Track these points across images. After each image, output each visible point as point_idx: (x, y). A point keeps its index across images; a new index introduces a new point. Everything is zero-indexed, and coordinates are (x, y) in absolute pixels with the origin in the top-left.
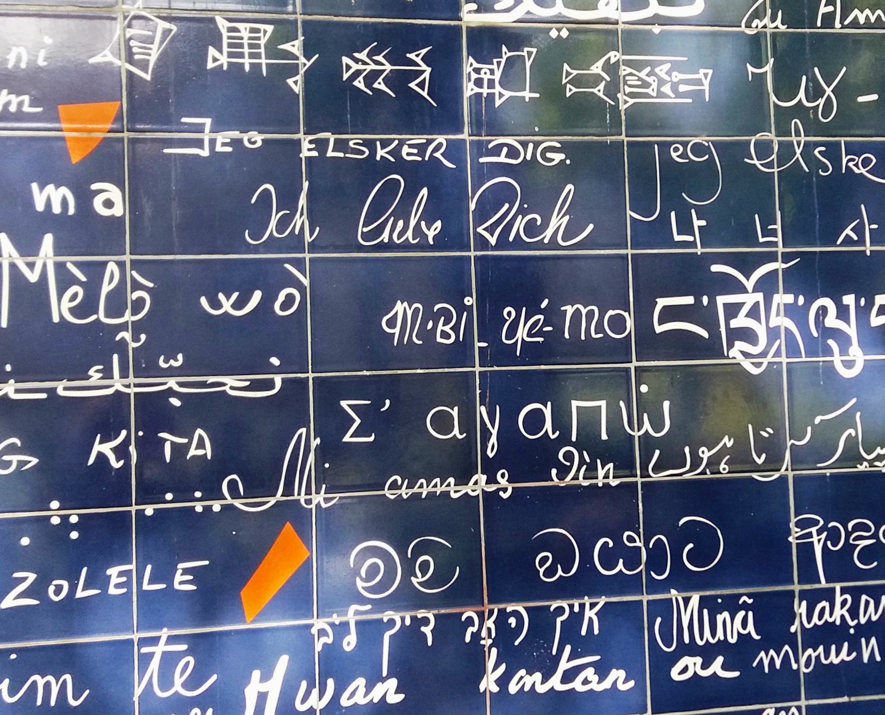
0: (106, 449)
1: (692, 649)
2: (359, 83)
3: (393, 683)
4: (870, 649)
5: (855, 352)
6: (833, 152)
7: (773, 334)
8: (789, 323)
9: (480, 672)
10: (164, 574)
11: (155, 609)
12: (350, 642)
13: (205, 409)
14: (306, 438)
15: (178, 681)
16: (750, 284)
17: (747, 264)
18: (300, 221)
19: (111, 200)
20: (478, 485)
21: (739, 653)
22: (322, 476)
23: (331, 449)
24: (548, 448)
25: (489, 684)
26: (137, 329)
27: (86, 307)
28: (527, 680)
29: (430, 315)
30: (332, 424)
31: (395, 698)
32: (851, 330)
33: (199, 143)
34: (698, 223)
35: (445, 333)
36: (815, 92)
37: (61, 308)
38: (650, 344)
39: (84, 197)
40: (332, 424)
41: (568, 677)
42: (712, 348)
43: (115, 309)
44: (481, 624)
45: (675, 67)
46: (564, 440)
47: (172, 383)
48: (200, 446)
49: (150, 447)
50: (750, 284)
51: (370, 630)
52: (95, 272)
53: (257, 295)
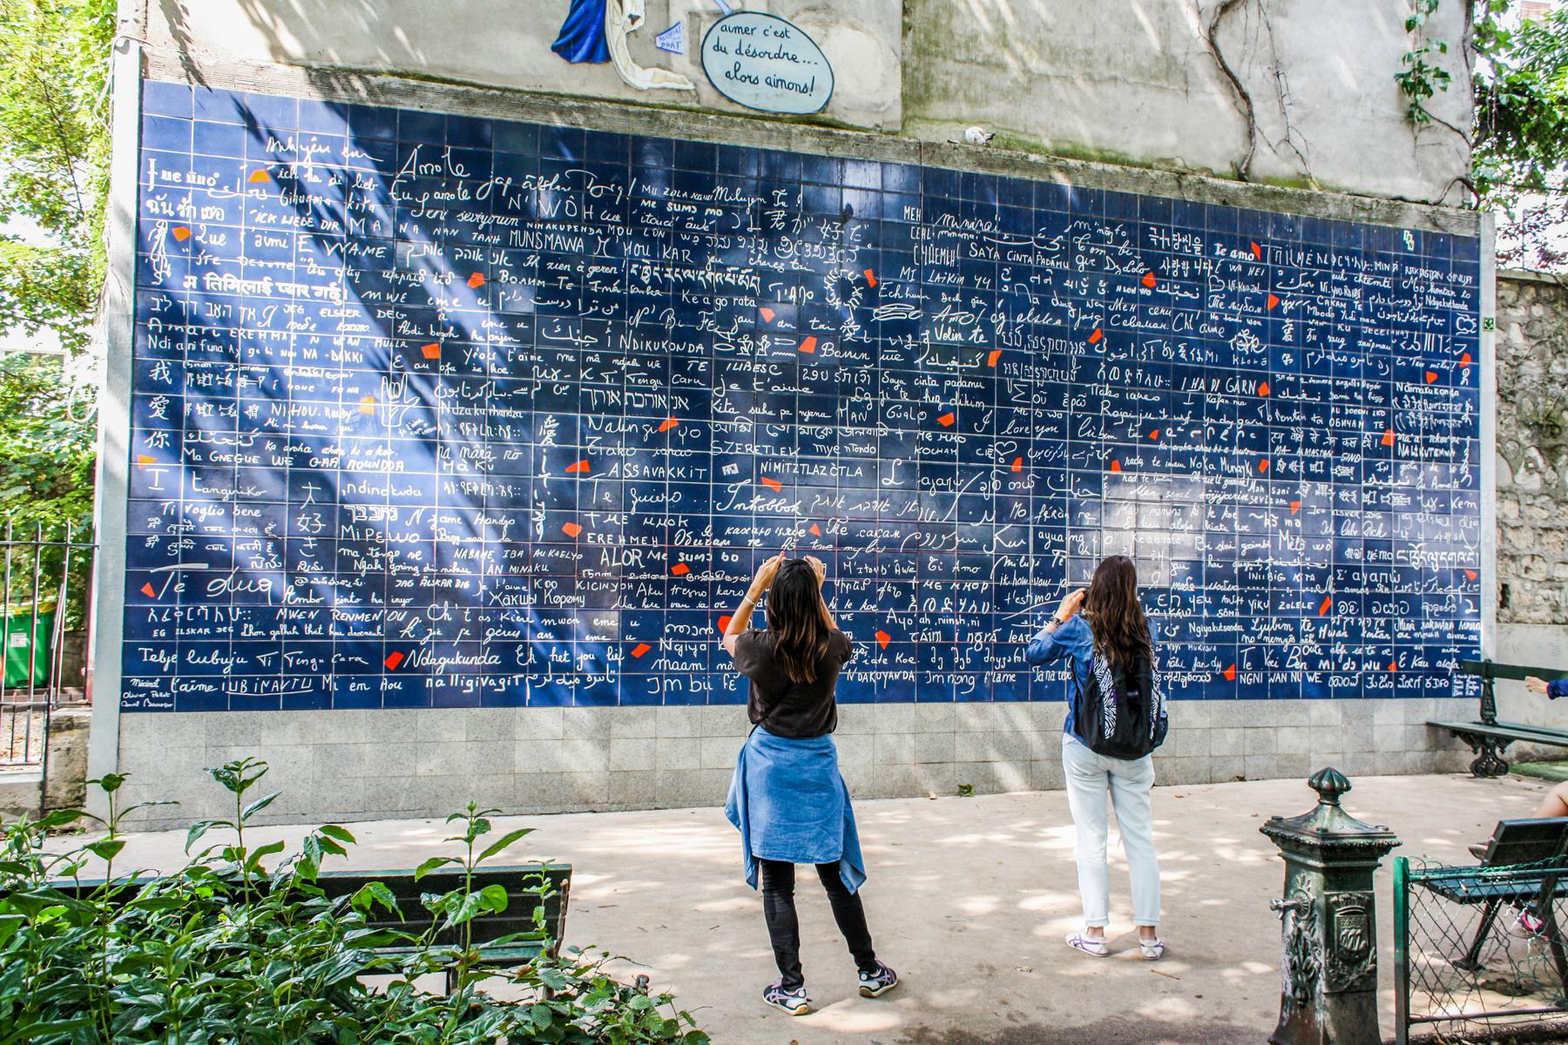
4: (1437, 635)
11: (1305, 612)
14: (1331, 578)
19: (1298, 523)
20: (1362, 591)
21: (1411, 633)
28: (1370, 635)
30: (1336, 575)
35: (1357, 556)
37: (1289, 546)
38: (1397, 561)
40: (1336, 575)
44: (1362, 622)
48: (1312, 578)
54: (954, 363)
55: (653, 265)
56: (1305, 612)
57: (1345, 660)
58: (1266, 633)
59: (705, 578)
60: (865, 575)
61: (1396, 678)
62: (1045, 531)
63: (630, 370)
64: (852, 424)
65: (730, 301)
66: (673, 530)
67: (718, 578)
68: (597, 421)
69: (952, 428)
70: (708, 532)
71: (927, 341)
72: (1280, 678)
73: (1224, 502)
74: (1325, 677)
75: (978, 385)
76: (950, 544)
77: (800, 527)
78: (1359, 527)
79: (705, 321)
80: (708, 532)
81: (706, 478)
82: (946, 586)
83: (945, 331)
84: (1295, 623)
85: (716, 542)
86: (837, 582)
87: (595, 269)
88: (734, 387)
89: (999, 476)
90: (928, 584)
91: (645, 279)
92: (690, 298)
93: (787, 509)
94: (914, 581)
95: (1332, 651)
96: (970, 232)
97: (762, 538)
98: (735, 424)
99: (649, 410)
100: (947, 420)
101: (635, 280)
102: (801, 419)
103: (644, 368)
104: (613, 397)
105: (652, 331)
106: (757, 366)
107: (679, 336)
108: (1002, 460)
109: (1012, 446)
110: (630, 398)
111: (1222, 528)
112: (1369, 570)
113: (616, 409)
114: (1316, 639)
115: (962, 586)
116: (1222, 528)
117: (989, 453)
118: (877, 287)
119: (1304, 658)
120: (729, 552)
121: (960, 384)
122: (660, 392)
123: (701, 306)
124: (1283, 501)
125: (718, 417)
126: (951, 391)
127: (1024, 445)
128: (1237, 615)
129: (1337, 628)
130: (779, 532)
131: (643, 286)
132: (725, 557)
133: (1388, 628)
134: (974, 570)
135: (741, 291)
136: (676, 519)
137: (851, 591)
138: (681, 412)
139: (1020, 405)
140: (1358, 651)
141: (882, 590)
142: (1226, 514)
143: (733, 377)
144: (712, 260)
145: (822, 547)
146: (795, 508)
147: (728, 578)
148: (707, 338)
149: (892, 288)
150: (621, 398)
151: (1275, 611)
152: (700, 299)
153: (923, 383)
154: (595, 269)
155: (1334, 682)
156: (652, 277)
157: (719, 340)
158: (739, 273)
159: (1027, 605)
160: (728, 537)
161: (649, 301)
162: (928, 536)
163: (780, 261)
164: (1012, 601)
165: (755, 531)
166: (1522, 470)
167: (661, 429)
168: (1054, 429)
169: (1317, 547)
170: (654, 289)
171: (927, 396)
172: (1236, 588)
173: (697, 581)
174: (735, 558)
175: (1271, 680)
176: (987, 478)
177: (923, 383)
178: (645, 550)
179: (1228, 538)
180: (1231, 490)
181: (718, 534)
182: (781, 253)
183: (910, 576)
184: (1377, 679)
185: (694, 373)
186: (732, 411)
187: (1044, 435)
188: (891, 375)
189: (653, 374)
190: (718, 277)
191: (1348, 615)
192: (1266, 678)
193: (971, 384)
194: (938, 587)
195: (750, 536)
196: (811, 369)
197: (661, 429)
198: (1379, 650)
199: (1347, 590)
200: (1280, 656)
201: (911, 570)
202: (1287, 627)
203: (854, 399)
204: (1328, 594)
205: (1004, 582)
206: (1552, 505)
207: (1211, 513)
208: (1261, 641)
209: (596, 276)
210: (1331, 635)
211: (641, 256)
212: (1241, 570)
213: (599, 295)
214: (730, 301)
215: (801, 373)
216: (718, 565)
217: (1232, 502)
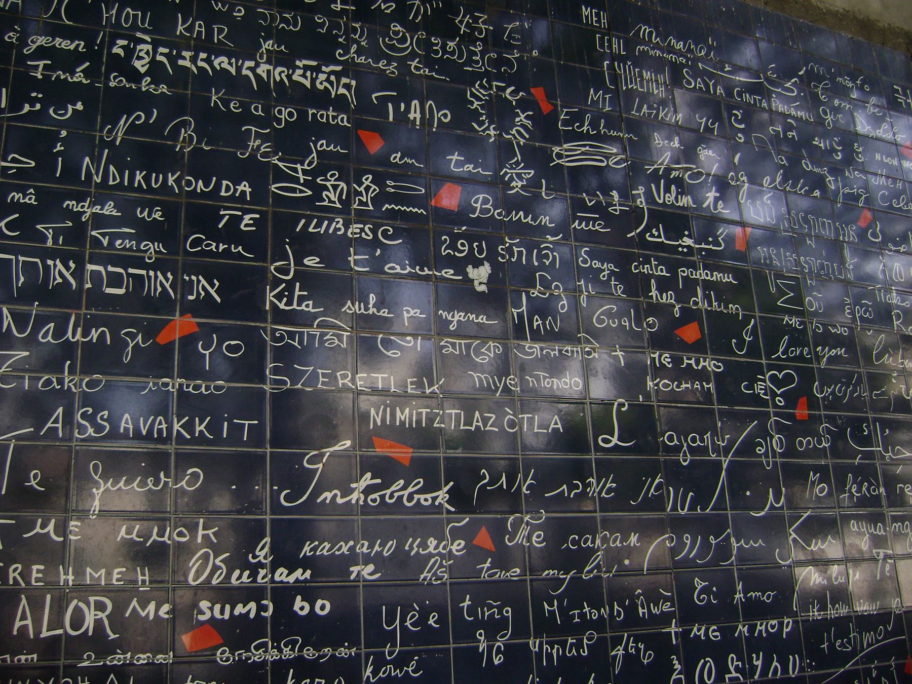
54: (688, 241)
55: (155, 44)
59: (257, 656)
60: (586, 624)
63: (99, 221)
64: (536, 336)
65: (303, 114)
66: (185, 550)
67: (288, 653)
68: (20, 320)
69: (698, 348)
70: (263, 553)
71: (641, 202)
75: (728, 279)
76: (724, 551)
77: (456, 534)
79: (254, 143)
80: (263, 553)
81: (257, 434)
82: (727, 631)
83: (667, 190)
85: (281, 575)
86: (534, 644)
87: (42, 41)
88: (311, 262)
89: (780, 428)
90: (698, 631)
91: (141, 66)
92: (226, 103)
93: (425, 499)
94: (673, 629)
96: (679, 53)
97: (378, 561)
98: (316, 332)
99: (139, 298)
100: (690, 333)
101: (124, 66)
102: (443, 329)
103: (128, 219)
104: (60, 272)
105: (151, 154)
106: (355, 228)
107: (200, 166)
108: (780, 401)
109: (788, 379)
110: (95, 275)
113: (61, 297)
115: (752, 629)
117: (759, 388)
118: (555, 114)
120: (309, 593)
121: (701, 274)
122: (160, 265)
123: (247, 117)
125: (281, 317)
126: (690, 284)
127: (807, 376)
130: (413, 546)
131: (135, 76)
132: (300, 606)
134: (767, 597)
135: (322, 99)
136: (193, 528)
137: (562, 658)
138: (204, 306)
139: (791, 313)
141: (619, 651)
143: (306, 244)
144: (268, 45)
145: (500, 575)
146: (442, 496)
147: (309, 653)
148: (258, 173)
149: (578, 117)
150: (79, 274)
152: (245, 106)
153: (646, 269)
154: (42, 41)
156: (153, 63)
157: (280, 176)
158: (317, 70)
159: (854, 653)
160: (305, 563)
161: (145, 101)
162: (687, 539)
163: (390, 60)
164: (832, 646)
165: (363, 548)
167: (162, 338)
168: (841, 351)
170: (155, 82)
171: (654, 293)
173: (242, 663)
174: (324, 608)
176: (765, 434)
177: (646, 269)
178: (121, 596)
181: (285, 557)
182: (392, 48)
183: (665, 619)
185: (232, 232)
186: (308, 307)
187: (831, 360)
188: (592, 255)
189: (148, 231)
190: (279, 73)
193: (717, 276)
194: (714, 634)
195: (352, 558)
196: (454, 238)
197: (162, 338)
201: (666, 607)
203: (535, 293)
205: (815, 614)
209: (41, 52)
211: (135, 27)
213: (44, 84)
214: (303, 114)
215: (438, 244)
216: (286, 625)
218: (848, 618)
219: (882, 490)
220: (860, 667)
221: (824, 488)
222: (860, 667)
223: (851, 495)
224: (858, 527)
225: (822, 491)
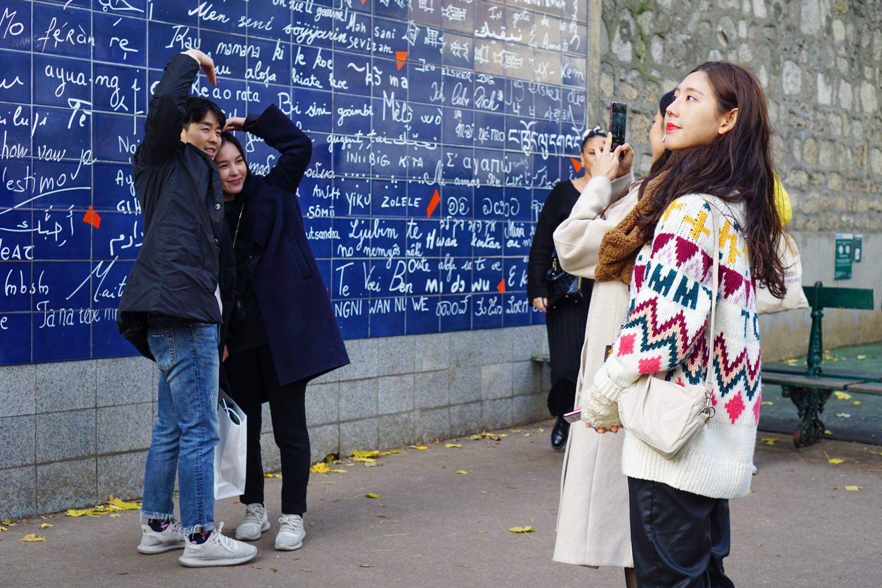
0: (402, 161)
1: (511, 238)
2: (454, 53)
3: (455, 241)
5: (547, 151)
6: (545, 89)
7: (532, 143)
8: (534, 141)
9: (471, 240)
10: (412, 202)
12: (447, 227)
13: (422, 152)
15: (415, 233)
16: (528, 127)
17: (528, 121)
18: (441, 95)
22: (444, 176)
23: (445, 169)
24: (487, 173)
25: (473, 244)
26: (409, 124)
27: (399, 117)
29: (466, 129)
30: (445, 161)
31: (456, 245)
32: (546, 145)
33: (421, 67)
34: (519, 107)
36: (542, 70)
39: (400, 81)
41: (488, 243)
42: (519, 147)
43: (405, 119)
45: (516, 57)
46: (490, 172)
47: (415, 142)
49: (411, 161)
50: (528, 127)
51: (452, 224)
52: (401, 104)
53: (432, 117)
56: (412, 211)
57: (454, 280)
58: (366, 242)
61: (503, 301)
62: (57, 64)
72: (383, 306)
73: (317, 41)
74: (432, 303)
78: (469, 95)
84: (401, 228)
95: (441, 267)
111: (312, 82)
112: (480, 154)
114: (424, 251)
116: (312, 82)
119: (408, 278)
124: (387, 49)
128: (332, 215)
129: (446, 234)
133: (498, 235)
140: (467, 266)
142: (319, 61)
151: (376, 209)
155: (442, 310)
159: (28, 194)
166: (617, 36)
169: (426, 120)
172: (330, 175)
175: (372, 310)
179: (323, 99)
180: (326, 24)
184: (486, 304)
191: (458, 216)
192: (366, 307)
198: (488, 263)
199: (458, 182)
200: (383, 275)
202: (391, 232)
204: (436, 184)
206: (640, 83)
207: (300, 57)
208: (361, 253)
210: (439, 244)
212: (338, 146)
217: (327, 43)
218: (26, 161)
219: (91, 40)
220: (32, 209)
221: (19, 28)
222: (32, 209)
223: (52, 40)
224: (54, 73)
225: (16, 29)
